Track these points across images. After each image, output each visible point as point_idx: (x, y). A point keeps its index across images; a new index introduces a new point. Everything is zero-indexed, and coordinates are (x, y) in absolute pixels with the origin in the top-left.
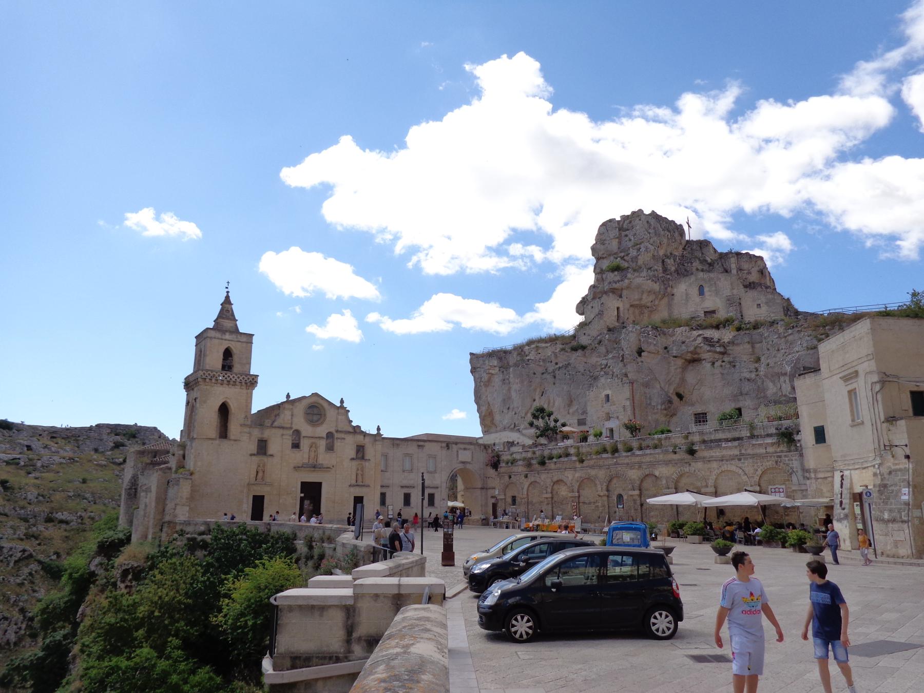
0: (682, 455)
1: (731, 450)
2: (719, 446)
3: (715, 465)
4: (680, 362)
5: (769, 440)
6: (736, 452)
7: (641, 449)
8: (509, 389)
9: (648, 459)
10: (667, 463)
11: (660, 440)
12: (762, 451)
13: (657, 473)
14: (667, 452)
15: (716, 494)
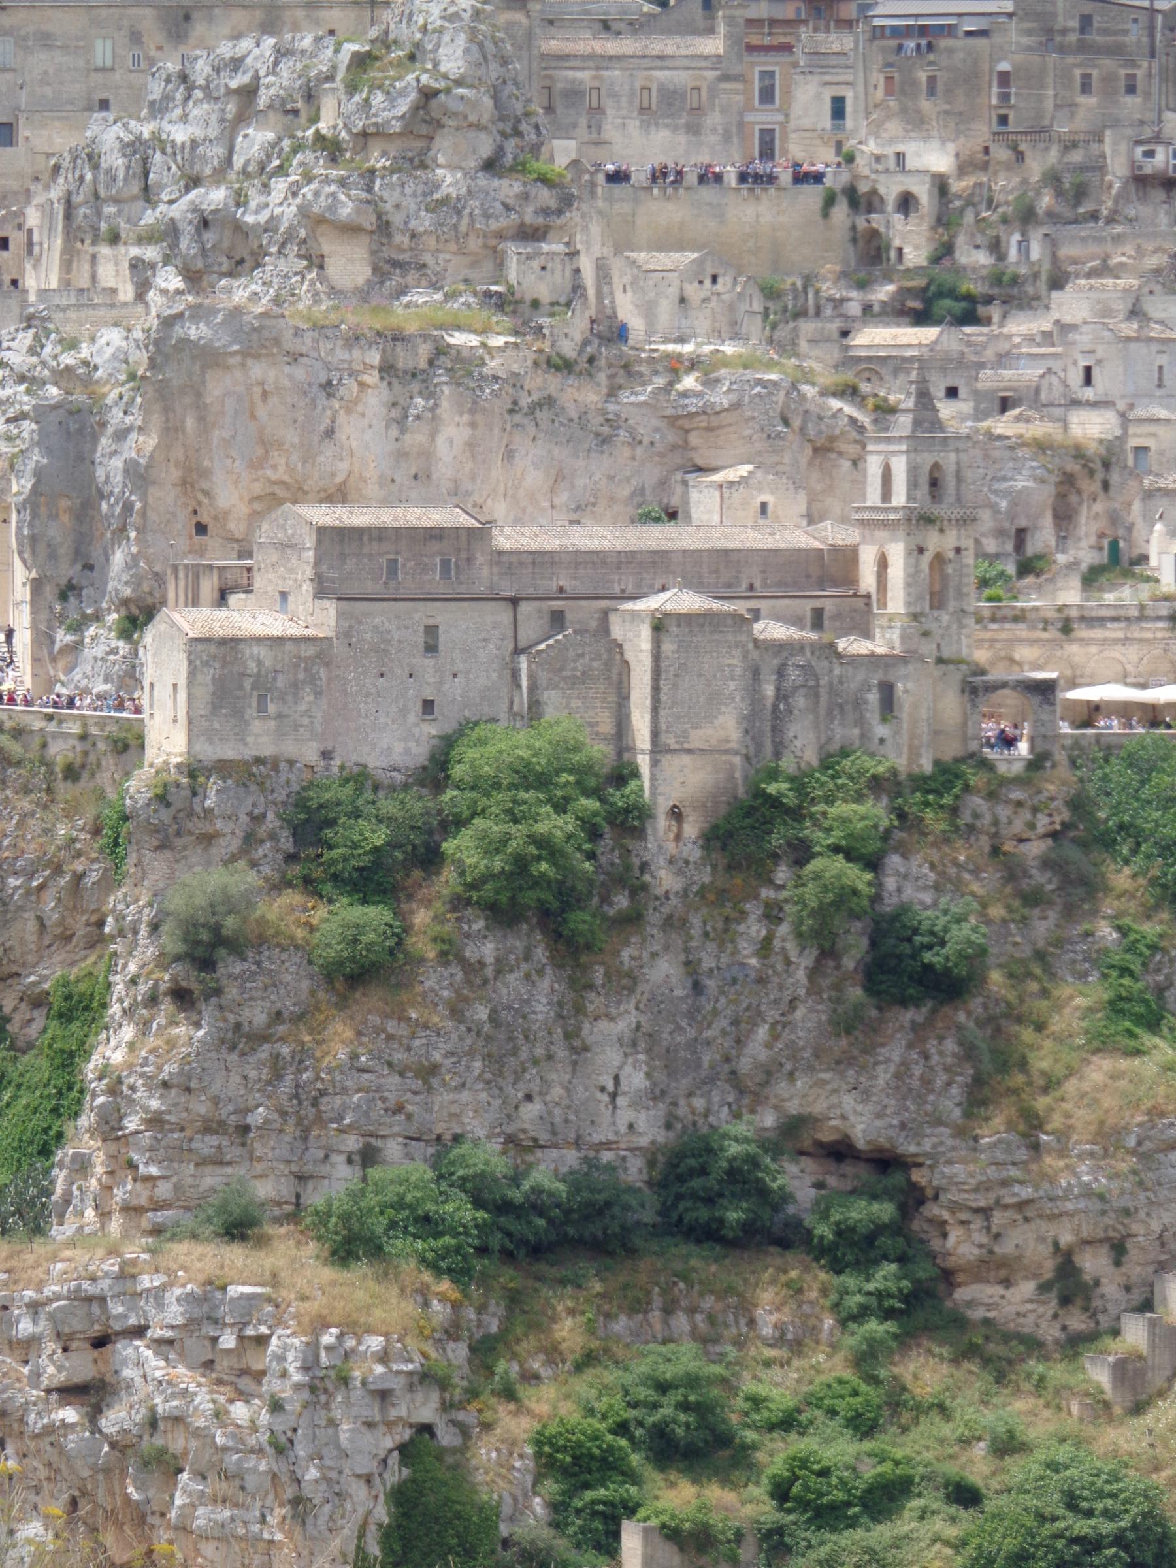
0: (1053, 633)
1: (1115, 631)
2: (1103, 626)
3: (1094, 649)
4: (809, 451)
5: (1160, 625)
6: (1120, 635)
7: (993, 620)
8: (433, 435)
9: (1004, 635)
10: (1032, 642)
11: (1023, 610)
12: (1149, 635)
13: (1017, 657)
14: (1033, 628)
15: (1144, 686)
